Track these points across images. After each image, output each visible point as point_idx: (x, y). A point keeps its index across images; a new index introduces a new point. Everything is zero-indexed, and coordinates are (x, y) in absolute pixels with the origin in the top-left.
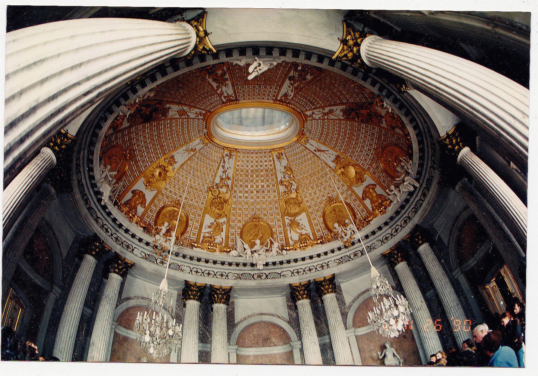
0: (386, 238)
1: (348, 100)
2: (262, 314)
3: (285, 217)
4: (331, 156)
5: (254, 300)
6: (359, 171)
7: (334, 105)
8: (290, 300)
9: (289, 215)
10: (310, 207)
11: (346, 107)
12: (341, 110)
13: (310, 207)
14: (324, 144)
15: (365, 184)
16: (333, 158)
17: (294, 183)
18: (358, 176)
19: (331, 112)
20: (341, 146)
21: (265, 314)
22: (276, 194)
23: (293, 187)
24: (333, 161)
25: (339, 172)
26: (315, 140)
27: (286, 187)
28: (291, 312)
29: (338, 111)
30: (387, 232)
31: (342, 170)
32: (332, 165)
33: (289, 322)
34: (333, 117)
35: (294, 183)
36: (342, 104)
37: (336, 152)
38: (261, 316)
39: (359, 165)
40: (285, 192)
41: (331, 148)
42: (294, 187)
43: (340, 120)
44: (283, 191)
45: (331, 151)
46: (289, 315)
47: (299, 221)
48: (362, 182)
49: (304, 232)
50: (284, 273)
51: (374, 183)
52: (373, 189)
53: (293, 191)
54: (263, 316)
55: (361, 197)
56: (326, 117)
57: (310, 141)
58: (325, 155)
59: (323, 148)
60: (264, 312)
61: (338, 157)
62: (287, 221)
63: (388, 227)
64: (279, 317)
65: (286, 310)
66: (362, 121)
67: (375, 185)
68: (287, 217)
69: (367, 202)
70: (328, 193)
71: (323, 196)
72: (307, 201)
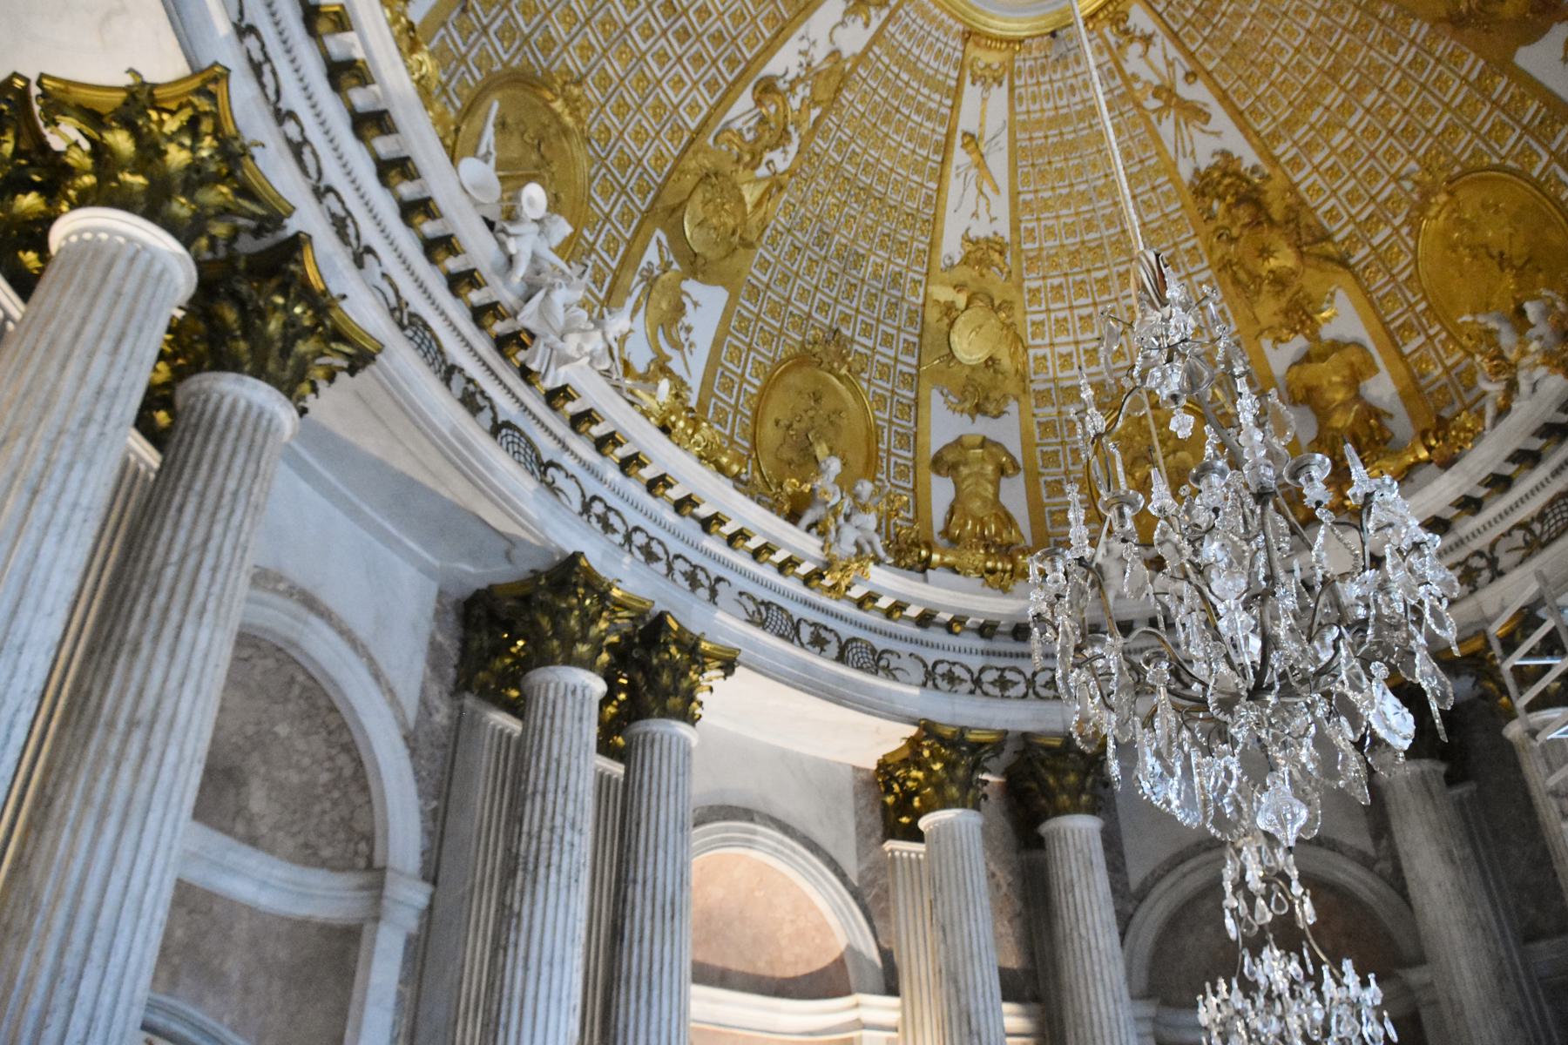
0: (951, 678)
1: (1295, 163)
2: (310, 602)
3: (659, 233)
4: (984, 217)
5: (304, 486)
6: (1006, 362)
7: (1237, 115)
8: (451, 618)
9: (676, 235)
10: (754, 293)
11: (1254, 170)
12: (1226, 154)
13: (754, 293)
14: (1014, 152)
15: (983, 427)
16: (981, 230)
17: (793, 149)
18: (984, 378)
19: (1197, 113)
20: (1050, 232)
21: (325, 614)
22: (705, 100)
23: (777, 156)
24: (966, 239)
25: (943, 294)
26: (1012, 108)
27: (763, 120)
28: (434, 689)
29: (1219, 138)
30: (964, 659)
31: (961, 300)
32: (951, 246)
33: (410, 739)
34: (1167, 128)
35: (793, 149)
36: (1264, 145)
37: (1015, 228)
38: (303, 612)
39: (1025, 349)
40: (740, 133)
41: (1014, 195)
42: (781, 160)
43: (1171, 168)
44: (738, 124)
45: (1001, 207)
46: (424, 702)
47: (689, 307)
48: (979, 409)
49: (676, 365)
50: (561, 481)
51: (1015, 449)
52: (1001, 471)
53: (762, 171)
54: (314, 620)
55: (935, 448)
56: (1152, 104)
57: (999, 95)
58: (972, 191)
59: (998, 163)
60: (328, 598)
61: (995, 245)
62: (652, 255)
63: (981, 644)
64: (377, 676)
65: (420, 666)
66: (1225, 265)
67: (1016, 468)
68: (664, 239)
69: (941, 492)
70: (846, 318)
71: (823, 308)
72: (764, 265)
